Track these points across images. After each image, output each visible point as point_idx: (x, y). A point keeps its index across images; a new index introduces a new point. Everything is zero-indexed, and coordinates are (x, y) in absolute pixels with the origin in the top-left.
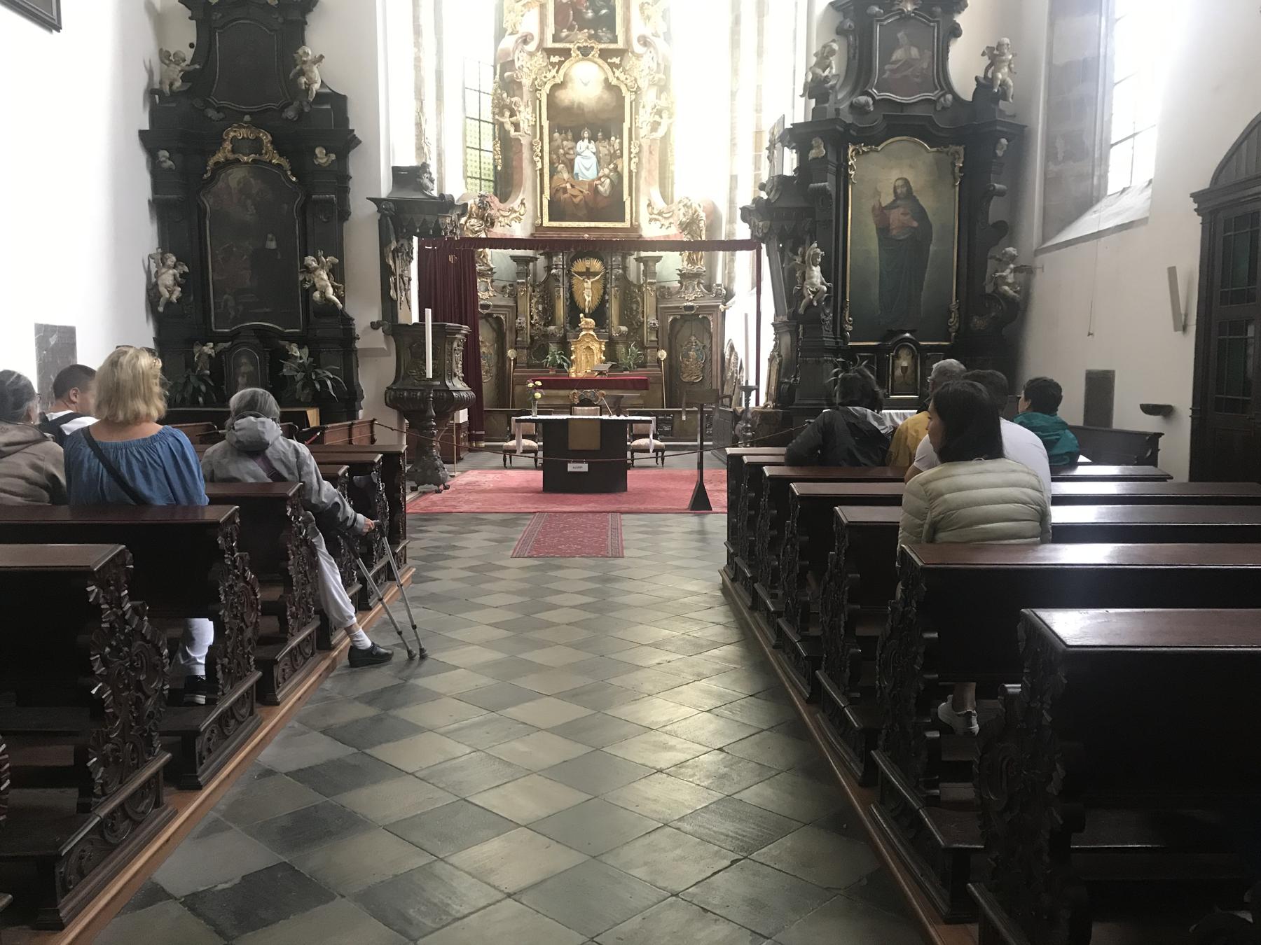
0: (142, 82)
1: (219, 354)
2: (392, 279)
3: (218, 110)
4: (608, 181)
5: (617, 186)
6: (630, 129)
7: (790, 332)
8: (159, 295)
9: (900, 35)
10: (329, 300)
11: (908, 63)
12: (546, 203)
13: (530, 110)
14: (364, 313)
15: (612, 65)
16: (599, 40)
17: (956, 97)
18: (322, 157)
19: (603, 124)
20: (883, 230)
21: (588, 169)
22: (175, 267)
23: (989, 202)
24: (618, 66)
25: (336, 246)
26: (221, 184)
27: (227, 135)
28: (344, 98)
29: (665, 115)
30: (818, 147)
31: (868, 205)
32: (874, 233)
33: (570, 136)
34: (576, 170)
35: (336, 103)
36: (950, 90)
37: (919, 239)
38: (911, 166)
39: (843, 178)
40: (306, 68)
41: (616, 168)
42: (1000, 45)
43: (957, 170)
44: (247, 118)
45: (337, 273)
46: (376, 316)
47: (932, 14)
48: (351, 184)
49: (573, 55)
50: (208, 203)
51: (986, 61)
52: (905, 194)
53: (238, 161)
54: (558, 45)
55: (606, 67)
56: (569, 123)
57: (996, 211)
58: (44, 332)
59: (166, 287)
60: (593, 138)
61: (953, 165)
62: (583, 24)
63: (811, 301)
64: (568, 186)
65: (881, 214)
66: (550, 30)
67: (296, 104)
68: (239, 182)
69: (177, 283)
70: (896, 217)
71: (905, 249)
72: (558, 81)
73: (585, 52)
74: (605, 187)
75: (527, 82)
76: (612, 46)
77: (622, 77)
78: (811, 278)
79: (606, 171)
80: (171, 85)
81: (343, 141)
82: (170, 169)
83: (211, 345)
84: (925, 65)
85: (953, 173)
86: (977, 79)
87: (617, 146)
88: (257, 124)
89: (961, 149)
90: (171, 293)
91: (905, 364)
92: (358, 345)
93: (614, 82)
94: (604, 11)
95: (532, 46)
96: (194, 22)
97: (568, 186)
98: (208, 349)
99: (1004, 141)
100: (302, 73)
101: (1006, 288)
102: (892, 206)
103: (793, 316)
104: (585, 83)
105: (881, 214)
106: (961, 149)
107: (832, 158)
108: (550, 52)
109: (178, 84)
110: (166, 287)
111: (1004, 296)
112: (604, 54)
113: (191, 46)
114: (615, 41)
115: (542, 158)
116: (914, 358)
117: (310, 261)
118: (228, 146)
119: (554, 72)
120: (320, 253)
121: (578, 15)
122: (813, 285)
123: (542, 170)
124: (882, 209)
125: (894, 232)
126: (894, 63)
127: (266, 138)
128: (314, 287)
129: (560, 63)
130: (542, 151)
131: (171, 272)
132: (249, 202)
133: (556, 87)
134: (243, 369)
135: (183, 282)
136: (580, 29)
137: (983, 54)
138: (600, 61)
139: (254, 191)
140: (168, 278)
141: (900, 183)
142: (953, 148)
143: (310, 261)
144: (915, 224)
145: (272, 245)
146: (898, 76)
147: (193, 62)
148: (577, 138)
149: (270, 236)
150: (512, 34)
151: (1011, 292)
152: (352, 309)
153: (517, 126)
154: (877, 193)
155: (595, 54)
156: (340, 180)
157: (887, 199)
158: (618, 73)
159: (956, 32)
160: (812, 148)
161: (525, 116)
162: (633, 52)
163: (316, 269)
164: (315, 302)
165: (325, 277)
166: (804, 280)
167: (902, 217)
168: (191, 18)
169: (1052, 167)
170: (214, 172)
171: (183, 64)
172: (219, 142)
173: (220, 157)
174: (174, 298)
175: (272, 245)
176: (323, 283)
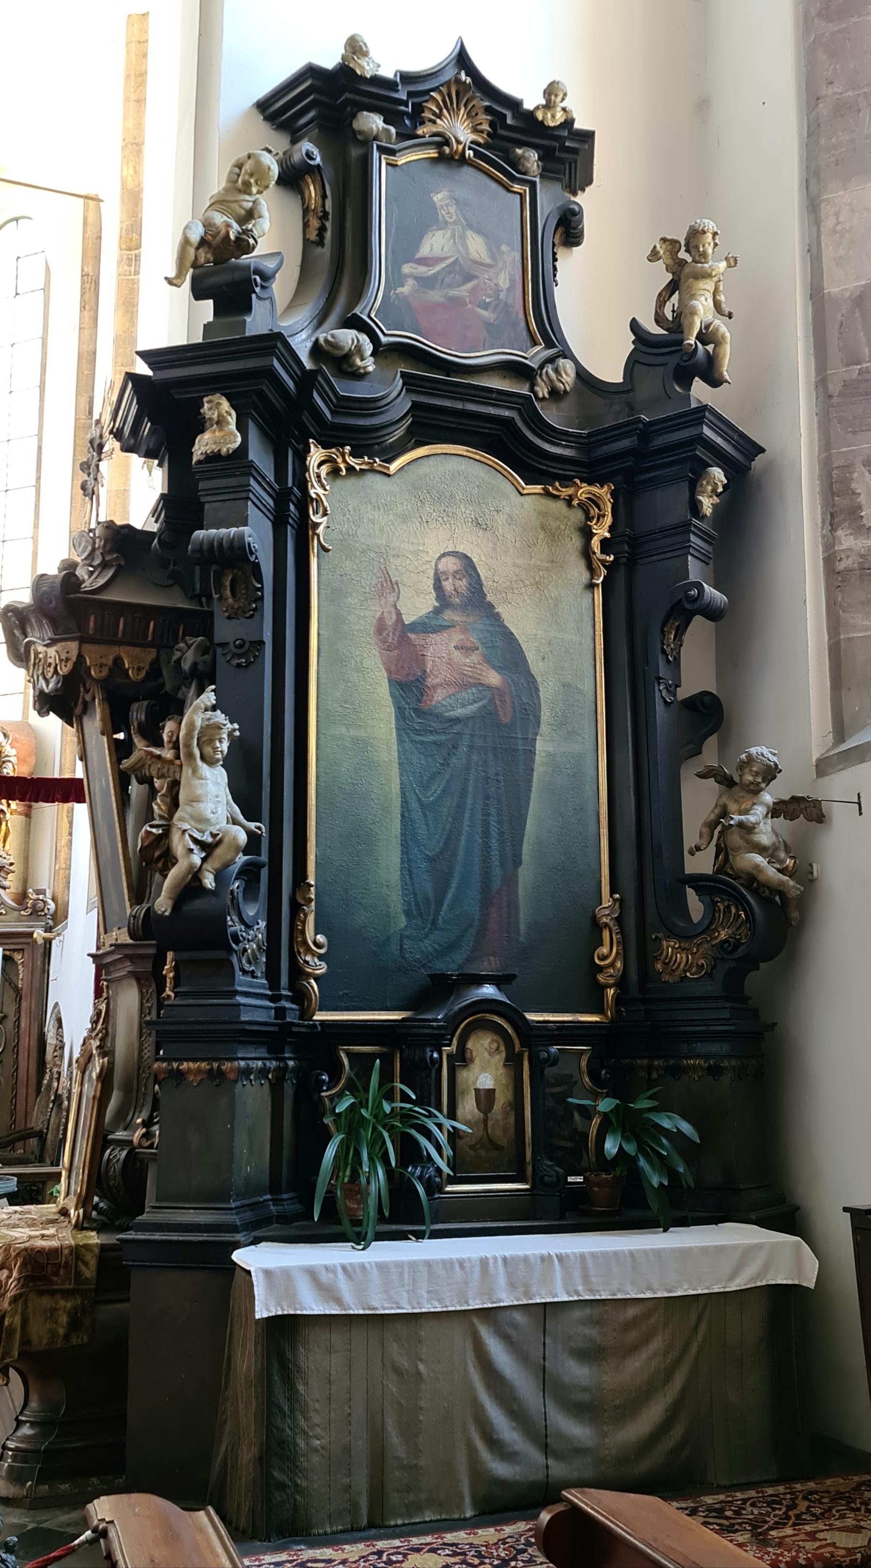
7: (139, 978)
11: (463, 271)
17: (583, 376)
20: (409, 687)
23: (680, 632)
30: (221, 422)
31: (364, 615)
32: (383, 690)
37: (507, 725)
39: (293, 516)
42: (695, 234)
43: (595, 543)
47: (515, 163)
52: (467, 595)
61: (587, 534)
63: (196, 875)
65: (403, 643)
71: (471, 746)
78: (195, 800)
84: (503, 282)
85: (586, 553)
86: (635, 326)
89: (604, 492)
99: (718, 474)
101: (758, 859)
103: (147, 928)
105: (403, 643)
106: (604, 492)
107: (259, 456)
111: (752, 880)
116: (513, 1061)
122: (201, 820)
124: (404, 630)
125: (439, 696)
126: (424, 262)
137: (654, 256)
141: (450, 565)
142: (584, 491)
144: (494, 678)
146: (436, 296)
151: (771, 873)
154: (389, 586)
157: (417, 604)
160: (200, 426)
166: (174, 804)
167: (457, 656)
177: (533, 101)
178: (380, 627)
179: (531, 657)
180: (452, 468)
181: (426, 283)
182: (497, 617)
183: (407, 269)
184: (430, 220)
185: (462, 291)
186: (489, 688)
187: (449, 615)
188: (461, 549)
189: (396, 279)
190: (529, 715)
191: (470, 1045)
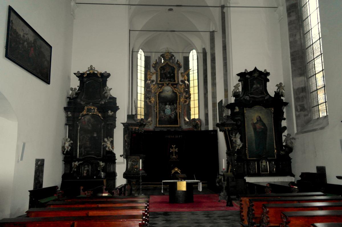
3: (84, 101)
4: (174, 115)
5: (176, 116)
6: (179, 102)
8: (65, 149)
9: (255, 82)
12: (157, 120)
13: (154, 98)
15: (174, 87)
16: (171, 81)
17: (270, 96)
19: (173, 101)
20: (255, 129)
21: (168, 112)
22: (69, 141)
24: (176, 87)
25: (112, 136)
28: (116, 98)
29: (188, 99)
33: (164, 104)
34: (165, 112)
35: (114, 99)
36: (268, 94)
37: (264, 131)
38: (261, 113)
41: (176, 112)
44: (91, 103)
48: (117, 119)
49: (165, 85)
51: (277, 88)
52: (260, 120)
54: (161, 83)
55: (173, 87)
56: (163, 101)
57: (284, 123)
58: (37, 161)
60: (169, 105)
62: (167, 78)
64: (163, 116)
65: (254, 125)
66: (159, 79)
69: (69, 146)
70: (258, 125)
72: (161, 91)
73: (168, 85)
74: (173, 117)
75: (153, 91)
76: (175, 83)
77: (177, 90)
79: (173, 112)
80: (73, 96)
83: (77, 162)
84: (261, 88)
86: (275, 92)
87: (176, 106)
88: (93, 105)
90: (68, 148)
91: (264, 164)
92: (116, 161)
93: (175, 91)
94: (172, 75)
95: (154, 83)
96: (79, 81)
97: (163, 116)
98: (77, 163)
100: (106, 93)
102: (256, 123)
104: (168, 91)
105: (254, 125)
108: (159, 84)
109: (74, 96)
112: (172, 85)
113: (78, 86)
114: (175, 81)
115: (157, 109)
117: (106, 140)
119: (160, 89)
120: (109, 137)
121: (166, 75)
123: (157, 113)
125: (258, 130)
126: (254, 88)
128: (106, 147)
129: (161, 87)
130: (157, 108)
131: (68, 143)
132: (90, 124)
133: (160, 93)
134: (86, 169)
135: (71, 145)
136: (166, 79)
137: (277, 85)
138: (171, 86)
140: (67, 144)
141: (258, 117)
143: (106, 140)
144: (263, 127)
147: (78, 90)
148: (166, 105)
149: (95, 133)
150: (149, 80)
152: (115, 151)
153: (150, 102)
154: (252, 120)
155: (170, 84)
156: (114, 118)
157: (255, 121)
158: (176, 89)
159: (268, 80)
160: (235, 109)
161: (153, 100)
162: (179, 84)
164: (106, 150)
165: (109, 143)
167: (259, 126)
168: (79, 80)
169: (298, 113)
171: (76, 91)
172: (83, 109)
174: (69, 150)
175: (95, 135)
177: (263, 71)
178: (252, 124)
179: (266, 125)
180: (257, 107)
181: (254, 90)
182: (262, 121)
183: (252, 89)
184: (253, 84)
185: (257, 90)
186: (262, 128)
187: (258, 122)
188: (259, 115)
189: (251, 90)
190: (267, 130)
191: (263, 161)
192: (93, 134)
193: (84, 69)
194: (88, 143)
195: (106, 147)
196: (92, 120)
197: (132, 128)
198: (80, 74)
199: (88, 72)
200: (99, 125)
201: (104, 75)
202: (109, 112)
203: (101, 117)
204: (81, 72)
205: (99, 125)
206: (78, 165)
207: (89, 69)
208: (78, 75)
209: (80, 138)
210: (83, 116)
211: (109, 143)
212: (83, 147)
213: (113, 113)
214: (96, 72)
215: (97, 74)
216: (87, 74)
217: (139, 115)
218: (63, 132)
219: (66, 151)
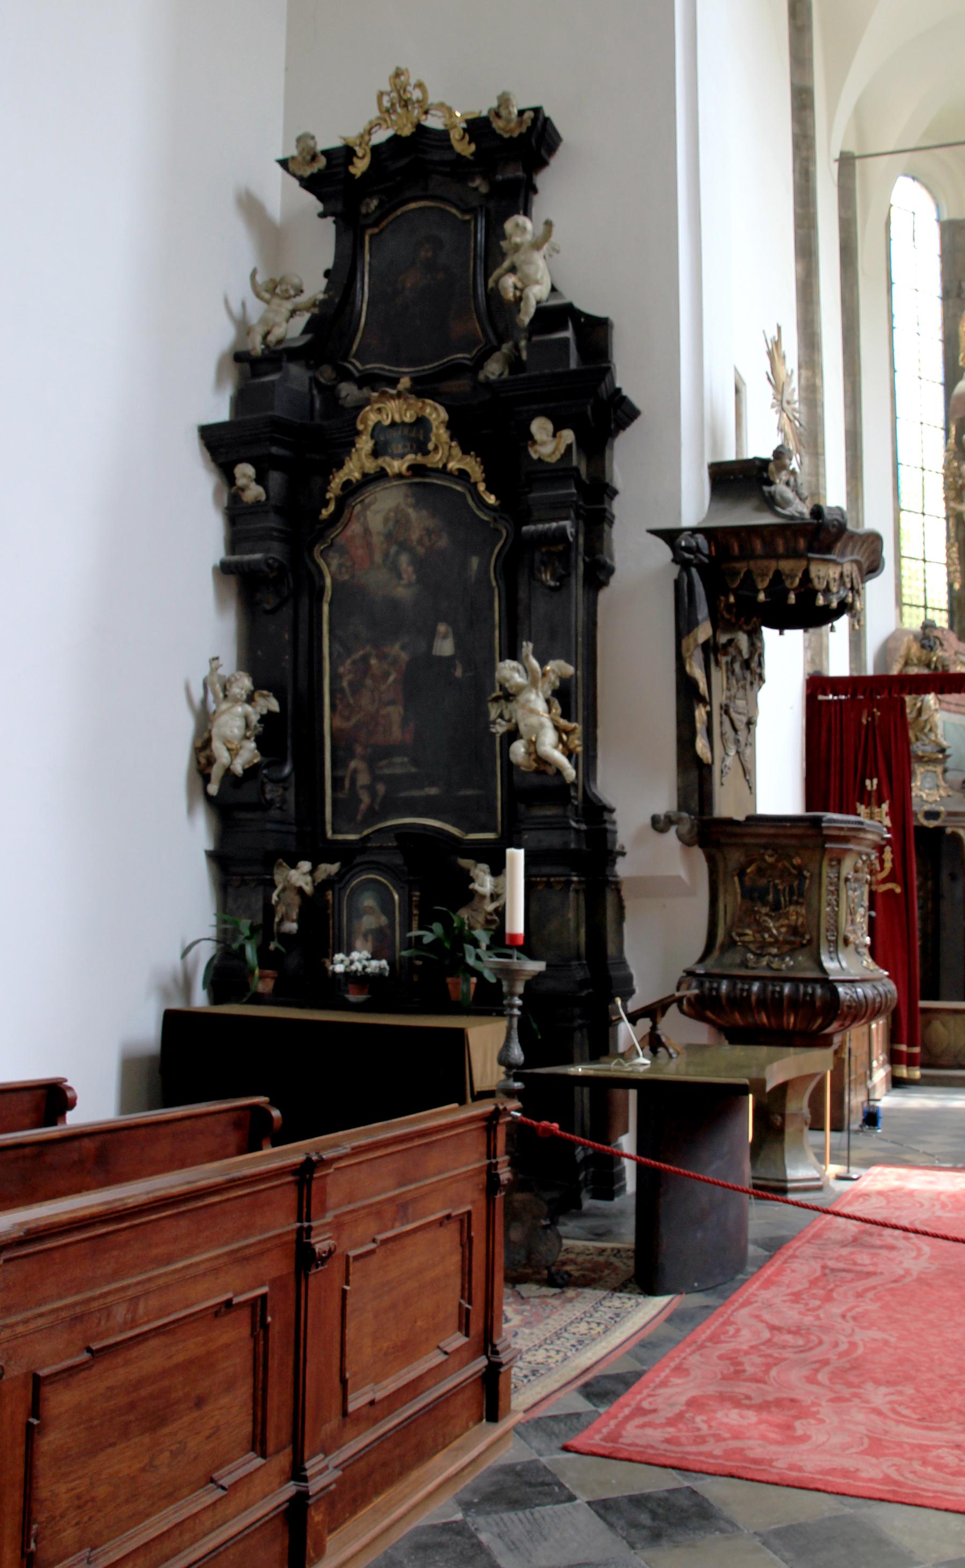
0: (223, 337)
1: (321, 887)
2: (700, 713)
10: (542, 761)
14: (637, 793)
18: (548, 441)
22: (250, 700)
26: (355, 528)
27: (364, 421)
35: (595, 333)
40: (517, 258)
45: (576, 702)
46: (664, 801)
50: (330, 571)
53: (382, 475)
59: (226, 741)
67: (506, 348)
68: (386, 520)
81: (602, 413)
82: (258, 503)
83: (305, 866)
88: (423, 388)
90: (233, 752)
92: (623, 868)
98: (300, 876)
110: (226, 741)
117: (510, 672)
118: (365, 444)
127: (437, 415)
131: (239, 709)
132: (404, 559)
135: (269, 734)
139: (415, 536)
143: (510, 672)
145: (445, 647)
149: (442, 628)
152: (610, 786)
156: (594, 500)
163: (521, 689)
165: (541, 706)
168: (322, 215)
170: (342, 502)
173: (352, 470)
174: (238, 768)
175: (445, 647)
176: (533, 720)
192: (431, 635)
193: (350, 119)
194: (395, 713)
195: (513, 735)
196: (419, 521)
197: (749, 573)
198: (322, 162)
199: (381, 136)
200: (475, 562)
201: (498, 125)
202: (540, 428)
203: (482, 487)
204: (327, 140)
205: (475, 562)
206: (308, 889)
207: (386, 103)
208: (307, 172)
209: (335, 678)
210: (351, 490)
211: (537, 701)
212: (359, 750)
213: (568, 436)
214: (434, 122)
215: (444, 136)
216: (376, 150)
217: (911, 605)
218: (201, 633)
219: (216, 772)
